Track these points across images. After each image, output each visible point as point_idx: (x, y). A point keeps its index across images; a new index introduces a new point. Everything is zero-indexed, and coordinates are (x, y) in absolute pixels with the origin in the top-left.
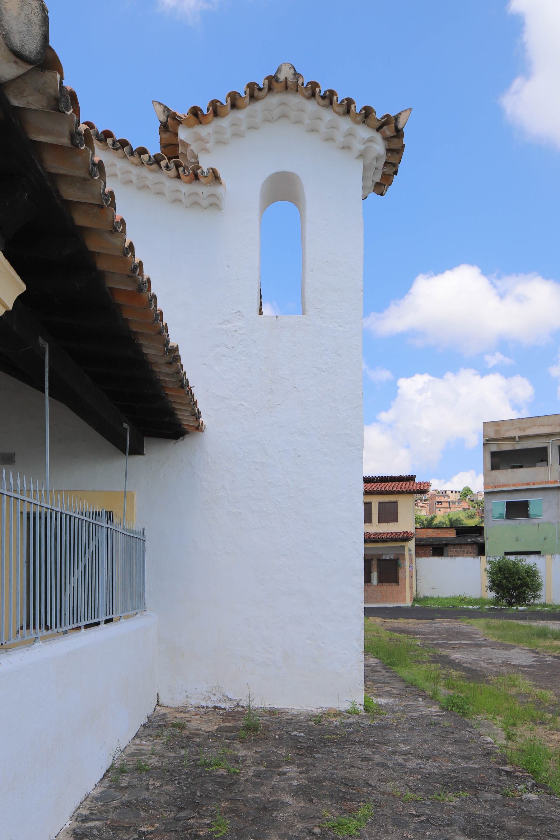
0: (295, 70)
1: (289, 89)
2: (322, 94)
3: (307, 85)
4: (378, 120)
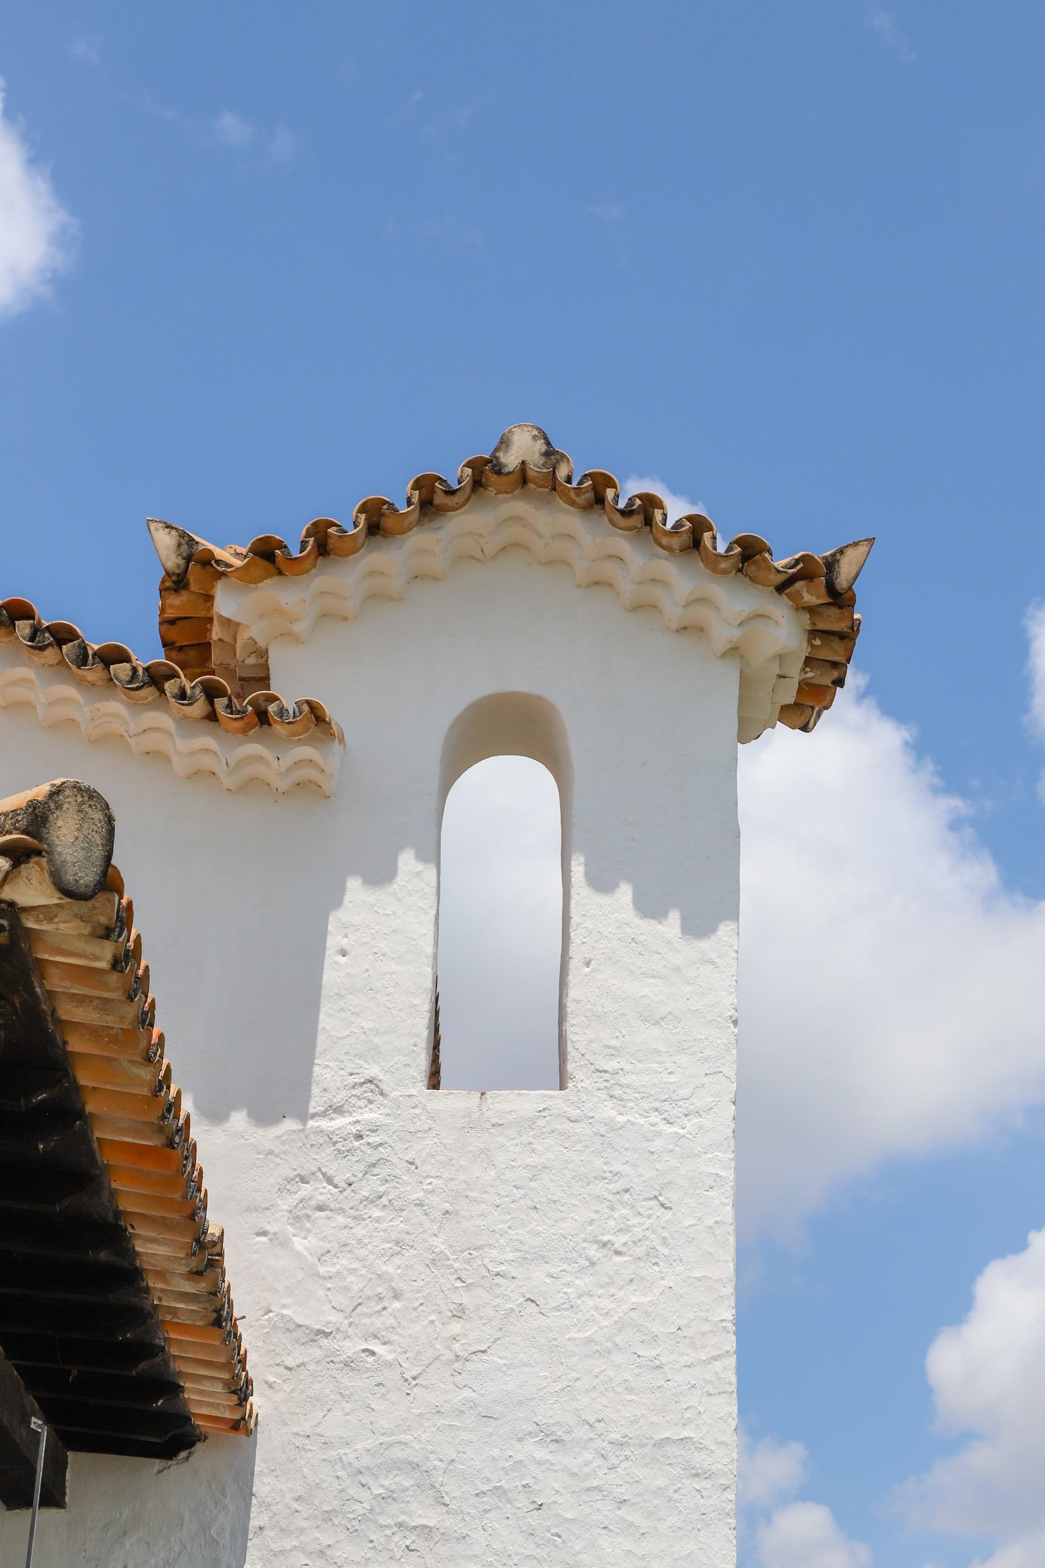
2: (621, 505)
3: (580, 483)
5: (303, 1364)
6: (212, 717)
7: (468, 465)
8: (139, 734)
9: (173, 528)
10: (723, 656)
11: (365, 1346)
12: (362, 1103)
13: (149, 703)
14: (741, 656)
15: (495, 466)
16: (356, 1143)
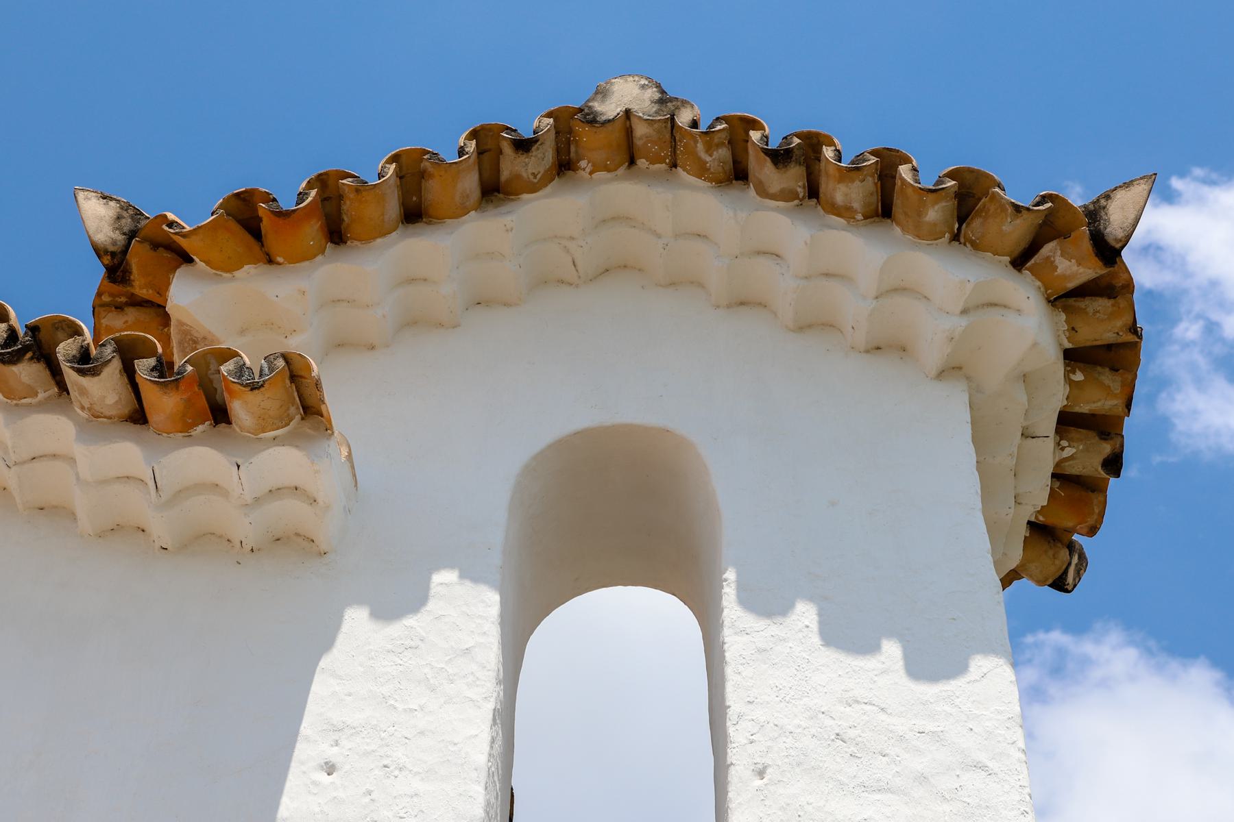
0: (663, 92)
1: (642, 163)
4: (1017, 209)
6: (138, 416)
8: (24, 462)
9: (112, 199)
10: (941, 375)
13: (40, 404)
14: (968, 378)
15: (588, 114)
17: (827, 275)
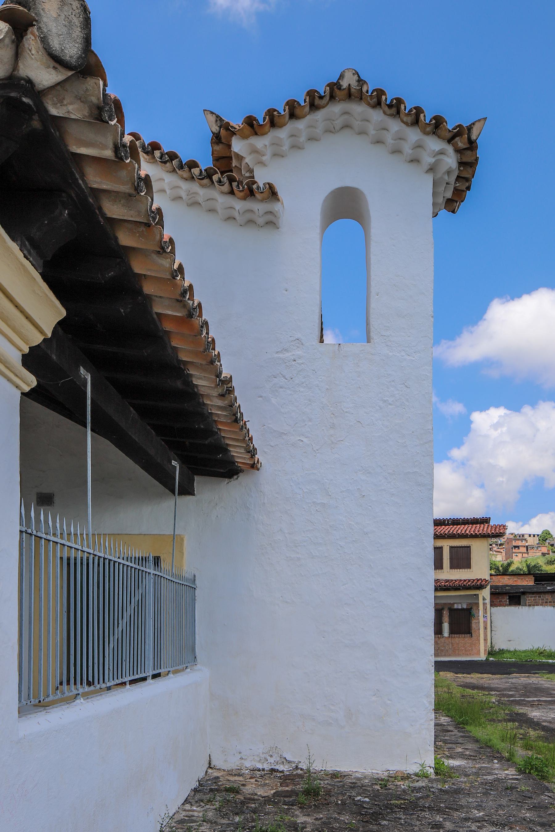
0: (359, 76)
1: (353, 97)
2: (388, 102)
3: (372, 93)
5: (277, 445)
7: (328, 85)
11: (299, 438)
12: (295, 348)
16: (293, 363)
17: (400, 139)
